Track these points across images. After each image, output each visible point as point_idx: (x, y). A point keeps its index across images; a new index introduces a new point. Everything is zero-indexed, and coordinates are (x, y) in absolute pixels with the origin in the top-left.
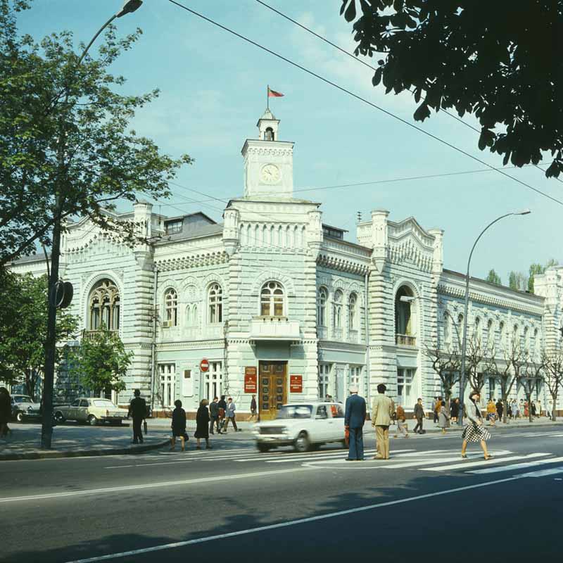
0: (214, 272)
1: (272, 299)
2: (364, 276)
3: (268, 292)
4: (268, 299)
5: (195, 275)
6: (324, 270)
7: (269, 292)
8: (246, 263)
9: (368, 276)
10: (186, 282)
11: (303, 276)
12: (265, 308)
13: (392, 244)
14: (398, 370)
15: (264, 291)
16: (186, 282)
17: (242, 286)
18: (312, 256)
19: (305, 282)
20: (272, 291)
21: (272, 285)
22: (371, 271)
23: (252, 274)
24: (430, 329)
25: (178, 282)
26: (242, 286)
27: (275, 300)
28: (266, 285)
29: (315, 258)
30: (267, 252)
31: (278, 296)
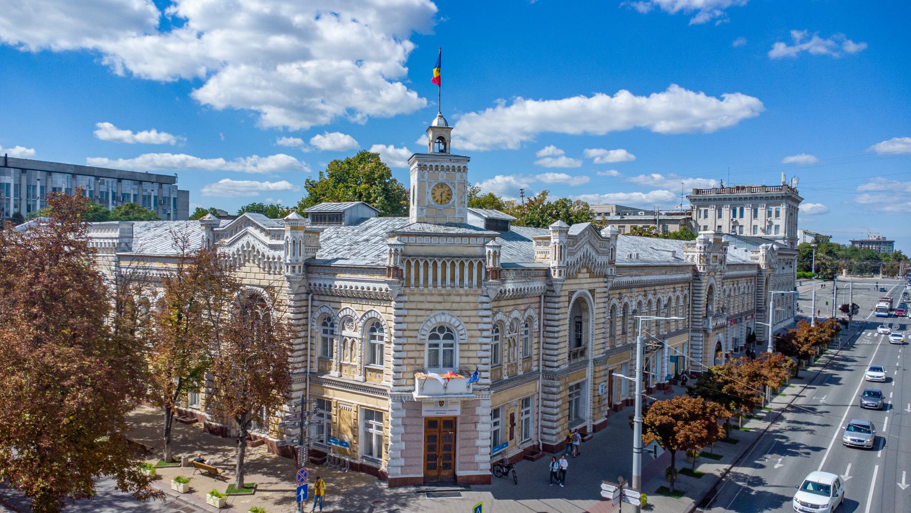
1: (441, 346)
2: (540, 297)
3: (437, 337)
8: (413, 306)
9: (545, 297)
11: (479, 320)
12: (434, 355)
15: (433, 337)
17: (407, 333)
18: (488, 296)
20: (441, 336)
21: (441, 329)
23: (420, 319)
27: (445, 345)
28: (434, 330)
31: (449, 342)
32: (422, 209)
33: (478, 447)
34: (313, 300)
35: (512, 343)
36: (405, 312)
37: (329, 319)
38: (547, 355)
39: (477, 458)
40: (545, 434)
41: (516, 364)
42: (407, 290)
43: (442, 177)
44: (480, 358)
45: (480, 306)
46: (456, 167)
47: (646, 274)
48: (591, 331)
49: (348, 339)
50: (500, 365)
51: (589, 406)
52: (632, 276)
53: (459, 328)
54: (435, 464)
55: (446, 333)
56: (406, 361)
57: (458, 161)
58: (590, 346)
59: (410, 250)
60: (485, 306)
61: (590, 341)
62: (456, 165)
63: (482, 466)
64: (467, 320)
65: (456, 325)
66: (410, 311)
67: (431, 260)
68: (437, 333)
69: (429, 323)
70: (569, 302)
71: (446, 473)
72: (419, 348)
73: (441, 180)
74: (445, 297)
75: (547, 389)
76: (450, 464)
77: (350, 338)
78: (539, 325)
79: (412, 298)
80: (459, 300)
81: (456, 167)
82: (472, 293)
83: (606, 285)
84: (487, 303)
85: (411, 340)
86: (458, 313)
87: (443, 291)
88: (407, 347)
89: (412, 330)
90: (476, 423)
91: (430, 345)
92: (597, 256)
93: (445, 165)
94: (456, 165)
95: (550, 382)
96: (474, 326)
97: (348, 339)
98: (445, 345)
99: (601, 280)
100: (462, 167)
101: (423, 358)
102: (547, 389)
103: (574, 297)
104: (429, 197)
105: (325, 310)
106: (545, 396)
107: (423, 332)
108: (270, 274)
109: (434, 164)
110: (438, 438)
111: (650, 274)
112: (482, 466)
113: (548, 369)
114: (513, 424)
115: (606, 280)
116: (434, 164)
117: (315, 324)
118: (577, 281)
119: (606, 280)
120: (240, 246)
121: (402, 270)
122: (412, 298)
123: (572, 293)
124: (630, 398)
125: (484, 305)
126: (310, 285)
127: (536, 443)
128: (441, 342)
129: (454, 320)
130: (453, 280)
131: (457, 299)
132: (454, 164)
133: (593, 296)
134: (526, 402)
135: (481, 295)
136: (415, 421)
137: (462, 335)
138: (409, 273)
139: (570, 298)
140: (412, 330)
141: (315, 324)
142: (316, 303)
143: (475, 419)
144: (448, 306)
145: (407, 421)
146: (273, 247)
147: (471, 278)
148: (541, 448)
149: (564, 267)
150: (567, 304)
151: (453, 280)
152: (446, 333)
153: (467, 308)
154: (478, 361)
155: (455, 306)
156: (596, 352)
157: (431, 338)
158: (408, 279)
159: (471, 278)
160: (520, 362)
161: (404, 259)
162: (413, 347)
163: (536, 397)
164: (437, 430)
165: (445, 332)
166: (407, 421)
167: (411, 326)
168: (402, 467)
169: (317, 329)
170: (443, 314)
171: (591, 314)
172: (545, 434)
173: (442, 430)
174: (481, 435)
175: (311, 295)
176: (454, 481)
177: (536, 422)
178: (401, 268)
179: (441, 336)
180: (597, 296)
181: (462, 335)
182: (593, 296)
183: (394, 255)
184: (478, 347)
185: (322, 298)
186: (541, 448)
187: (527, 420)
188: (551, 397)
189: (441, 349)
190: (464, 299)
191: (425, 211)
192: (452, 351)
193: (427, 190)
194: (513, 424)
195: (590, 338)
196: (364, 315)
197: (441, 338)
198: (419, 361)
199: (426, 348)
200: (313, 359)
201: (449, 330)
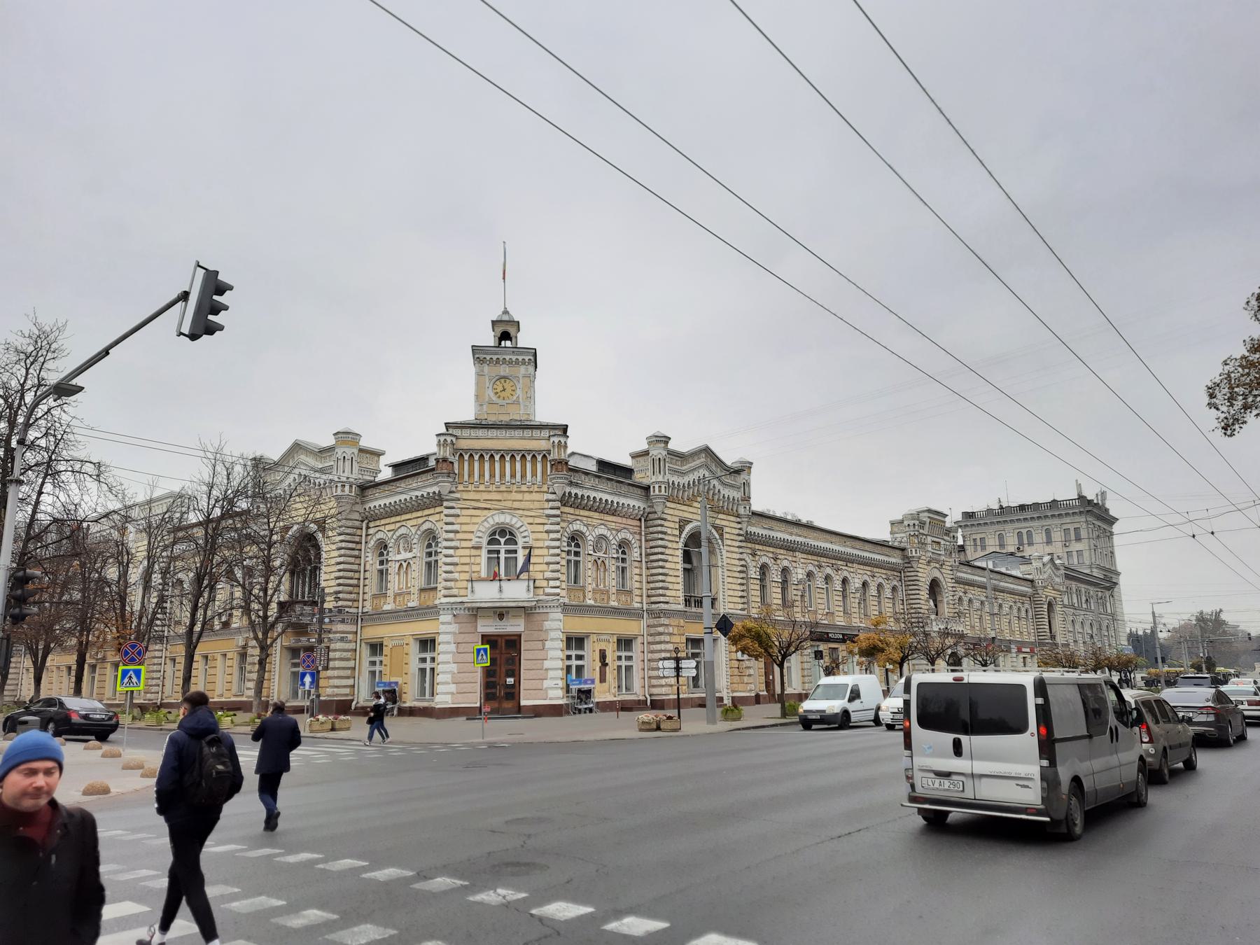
0: (430, 518)
1: (502, 552)
2: (640, 520)
4: (498, 552)
5: (409, 523)
6: (577, 512)
7: (499, 543)
10: (398, 534)
13: (676, 479)
14: (618, 640)
16: (398, 534)
18: (555, 493)
19: (547, 527)
20: (503, 540)
21: (503, 532)
22: (649, 513)
23: (475, 520)
24: (734, 587)
25: (390, 534)
26: (459, 536)
28: (494, 533)
29: (560, 493)
30: (495, 489)
32: (481, 405)
33: (546, 670)
34: (368, 528)
35: (599, 564)
36: (457, 511)
37: (386, 547)
38: (652, 589)
39: (546, 684)
40: (654, 686)
41: (608, 591)
42: (461, 487)
43: (504, 370)
44: (548, 564)
45: (547, 505)
46: (520, 360)
47: (814, 539)
48: (720, 577)
49: (403, 563)
50: (583, 587)
51: (724, 673)
52: (791, 534)
53: (521, 530)
54: (495, 693)
55: (507, 537)
56: (459, 568)
57: (522, 353)
58: (721, 597)
59: (463, 444)
60: (551, 504)
61: (721, 590)
62: (520, 358)
63: (552, 693)
64: (531, 520)
65: (518, 526)
66: (463, 511)
67: (487, 454)
68: (497, 537)
69: (485, 524)
70: (681, 533)
71: (508, 705)
72: (474, 552)
73: (502, 374)
74: (505, 494)
75: (652, 630)
76: (513, 693)
77: (405, 561)
78: (641, 555)
79: (465, 496)
80: (521, 498)
81: (520, 360)
82: (537, 489)
83: (739, 526)
84: (554, 501)
85: (464, 544)
86: (520, 512)
87: (503, 488)
88: (460, 552)
89: (466, 532)
90: (543, 641)
91: (490, 552)
92: (721, 488)
93: (508, 358)
94: (520, 358)
95: (655, 621)
96: (540, 528)
97: (403, 563)
98: (508, 552)
99: (732, 518)
100: (527, 360)
101: (479, 564)
102: (652, 630)
103: (688, 528)
104: (490, 393)
105: (380, 535)
106: (651, 639)
107: (480, 534)
108: (305, 475)
109: (495, 357)
110: (498, 662)
111: (818, 539)
112: (552, 693)
113: (653, 606)
114: (604, 664)
115: (739, 520)
116: (495, 357)
117: (369, 555)
118: (691, 509)
119: (739, 520)
120: (292, 479)
121: (452, 463)
122: (465, 496)
123: (683, 523)
124: (804, 692)
125: (551, 503)
126: (365, 509)
127: (642, 698)
128: (503, 548)
129: (514, 520)
130: (513, 475)
131: (519, 496)
132: (518, 357)
133: (721, 535)
134: (625, 643)
135: (548, 493)
136: (468, 638)
137: (525, 537)
138: (461, 468)
139: (681, 529)
140: (466, 532)
141: (369, 555)
142: (371, 531)
143: (543, 636)
144: (509, 504)
145: (461, 638)
146: (322, 471)
147: (534, 474)
148: (649, 704)
149: (664, 482)
150: (677, 533)
151: (513, 475)
152: (507, 537)
153: (531, 507)
154: (544, 567)
155: (516, 505)
156: (732, 606)
157: (490, 543)
158: (461, 475)
159: (534, 474)
160: (614, 590)
161: (456, 453)
162: (467, 552)
163: (640, 640)
164: (498, 651)
165: (504, 533)
166: (461, 638)
167: (465, 528)
168: (452, 694)
169: (370, 560)
170: (503, 513)
171: (719, 554)
172: (654, 686)
173: (504, 651)
174: (551, 654)
175: (366, 522)
176: (519, 711)
177: (641, 672)
178: (451, 459)
179: (503, 540)
180: (726, 536)
181: (525, 537)
182: (721, 535)
183: (443, 445)
184: (545, 552)
185: (378, 523)
186: (649, 704)
187: (629, 668)
188: (658, 638)
189: (502, 556)
190: (527, 497)
191: (485, 407)
192: (516, 558)
193: (487, 385)
194: (604, 664)
195: (721, 586)
196: (418, 529)
197: (502, 543)
198: (475, 568)
199: (484, 553)
200: (366, 597)
201: (511, 534)
